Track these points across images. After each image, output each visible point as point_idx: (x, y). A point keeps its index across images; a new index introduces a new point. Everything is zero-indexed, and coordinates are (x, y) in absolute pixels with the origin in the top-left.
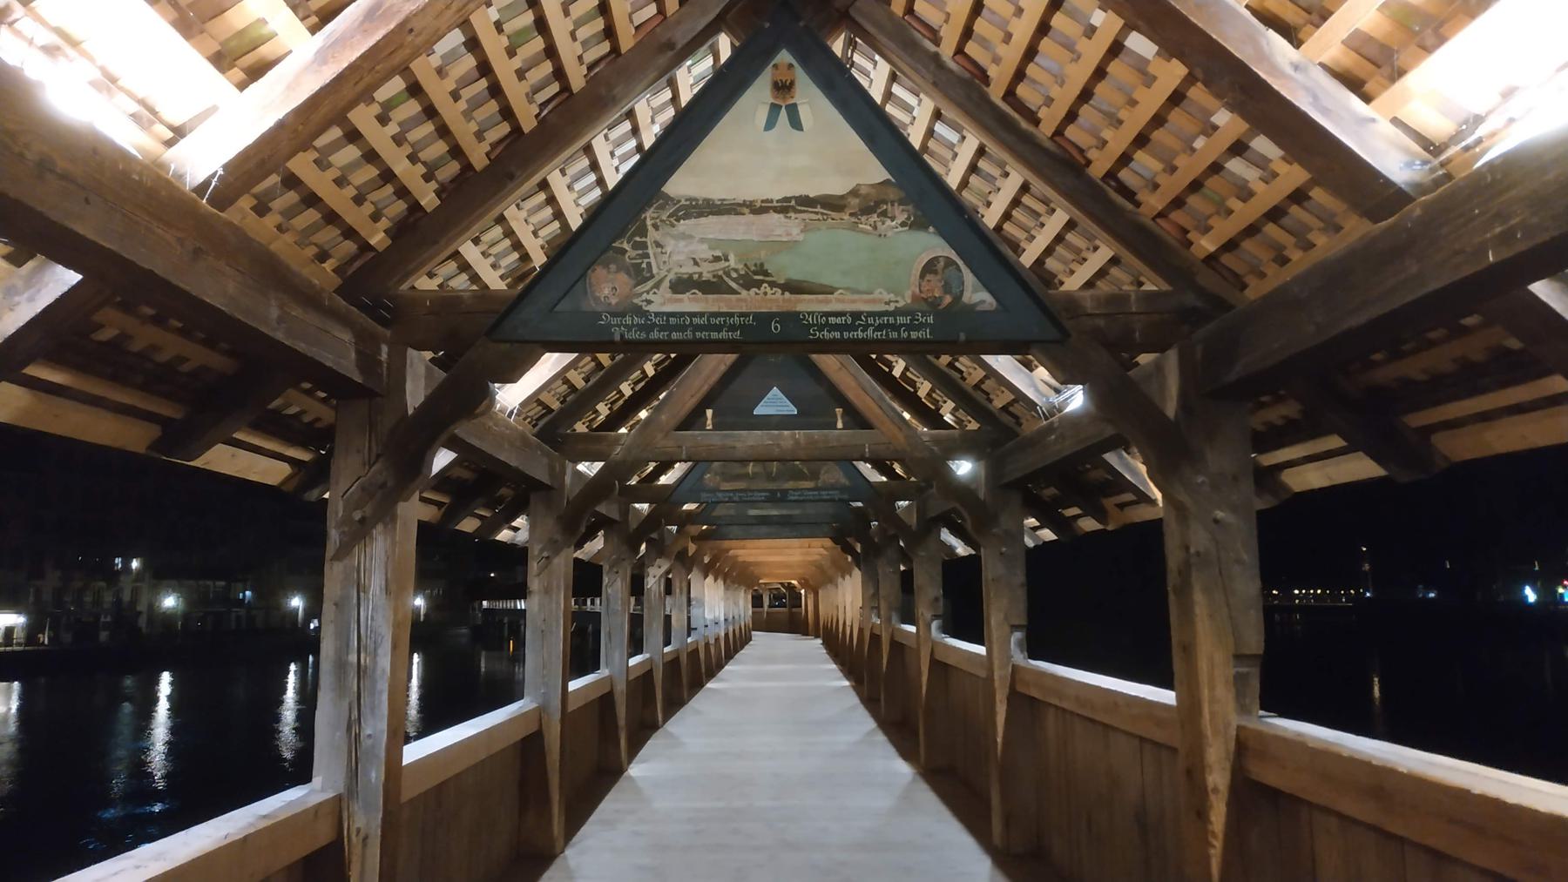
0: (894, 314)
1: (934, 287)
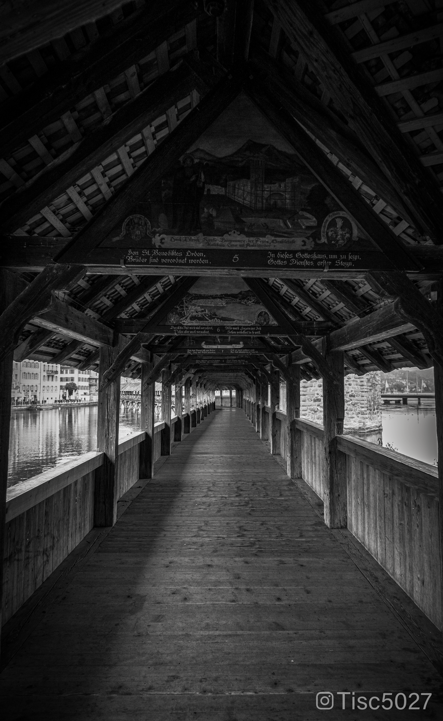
0: (251, 327)
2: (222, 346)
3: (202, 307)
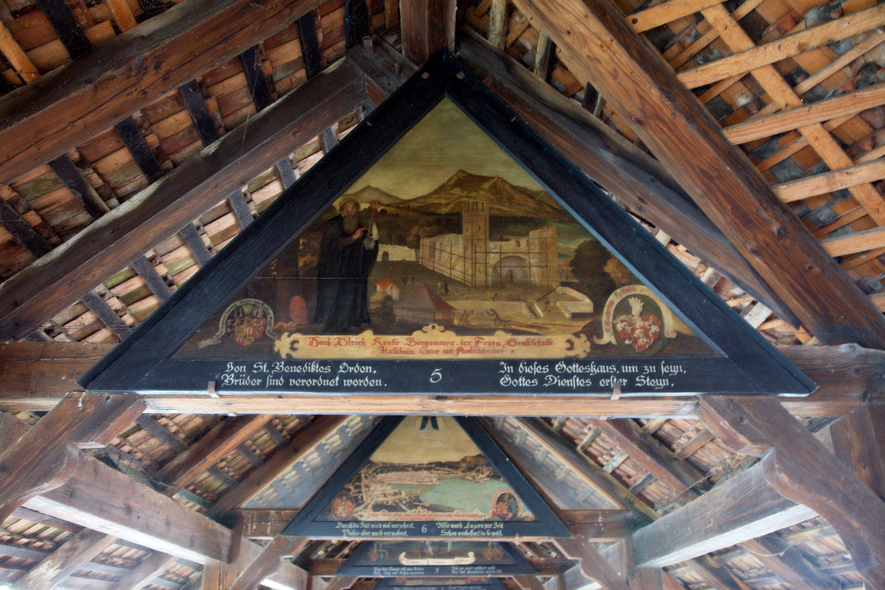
0: (485, 522)
1: (504, 506)
3: (395, 486)
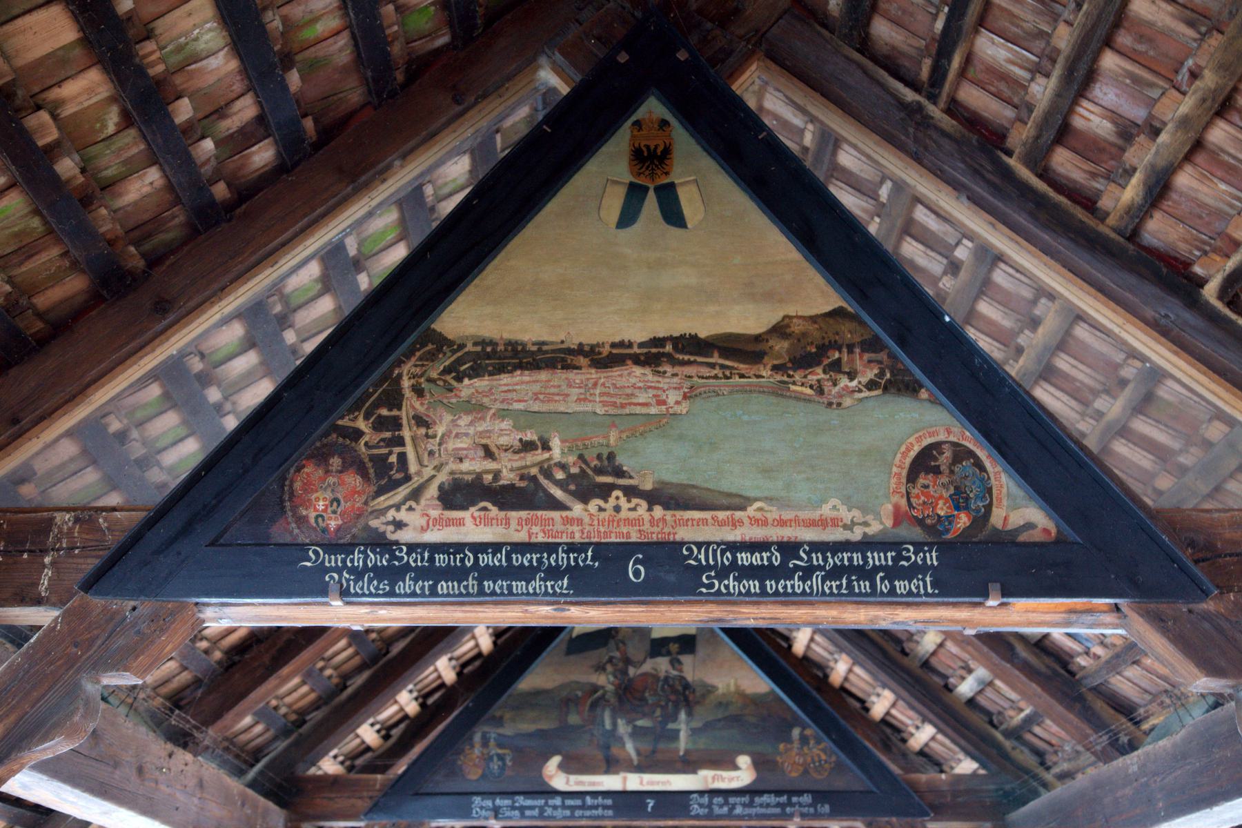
0: (866, 545)
2: (647, 777)
3: (523, 419)
